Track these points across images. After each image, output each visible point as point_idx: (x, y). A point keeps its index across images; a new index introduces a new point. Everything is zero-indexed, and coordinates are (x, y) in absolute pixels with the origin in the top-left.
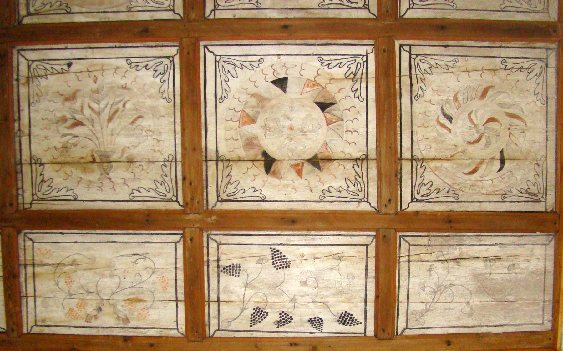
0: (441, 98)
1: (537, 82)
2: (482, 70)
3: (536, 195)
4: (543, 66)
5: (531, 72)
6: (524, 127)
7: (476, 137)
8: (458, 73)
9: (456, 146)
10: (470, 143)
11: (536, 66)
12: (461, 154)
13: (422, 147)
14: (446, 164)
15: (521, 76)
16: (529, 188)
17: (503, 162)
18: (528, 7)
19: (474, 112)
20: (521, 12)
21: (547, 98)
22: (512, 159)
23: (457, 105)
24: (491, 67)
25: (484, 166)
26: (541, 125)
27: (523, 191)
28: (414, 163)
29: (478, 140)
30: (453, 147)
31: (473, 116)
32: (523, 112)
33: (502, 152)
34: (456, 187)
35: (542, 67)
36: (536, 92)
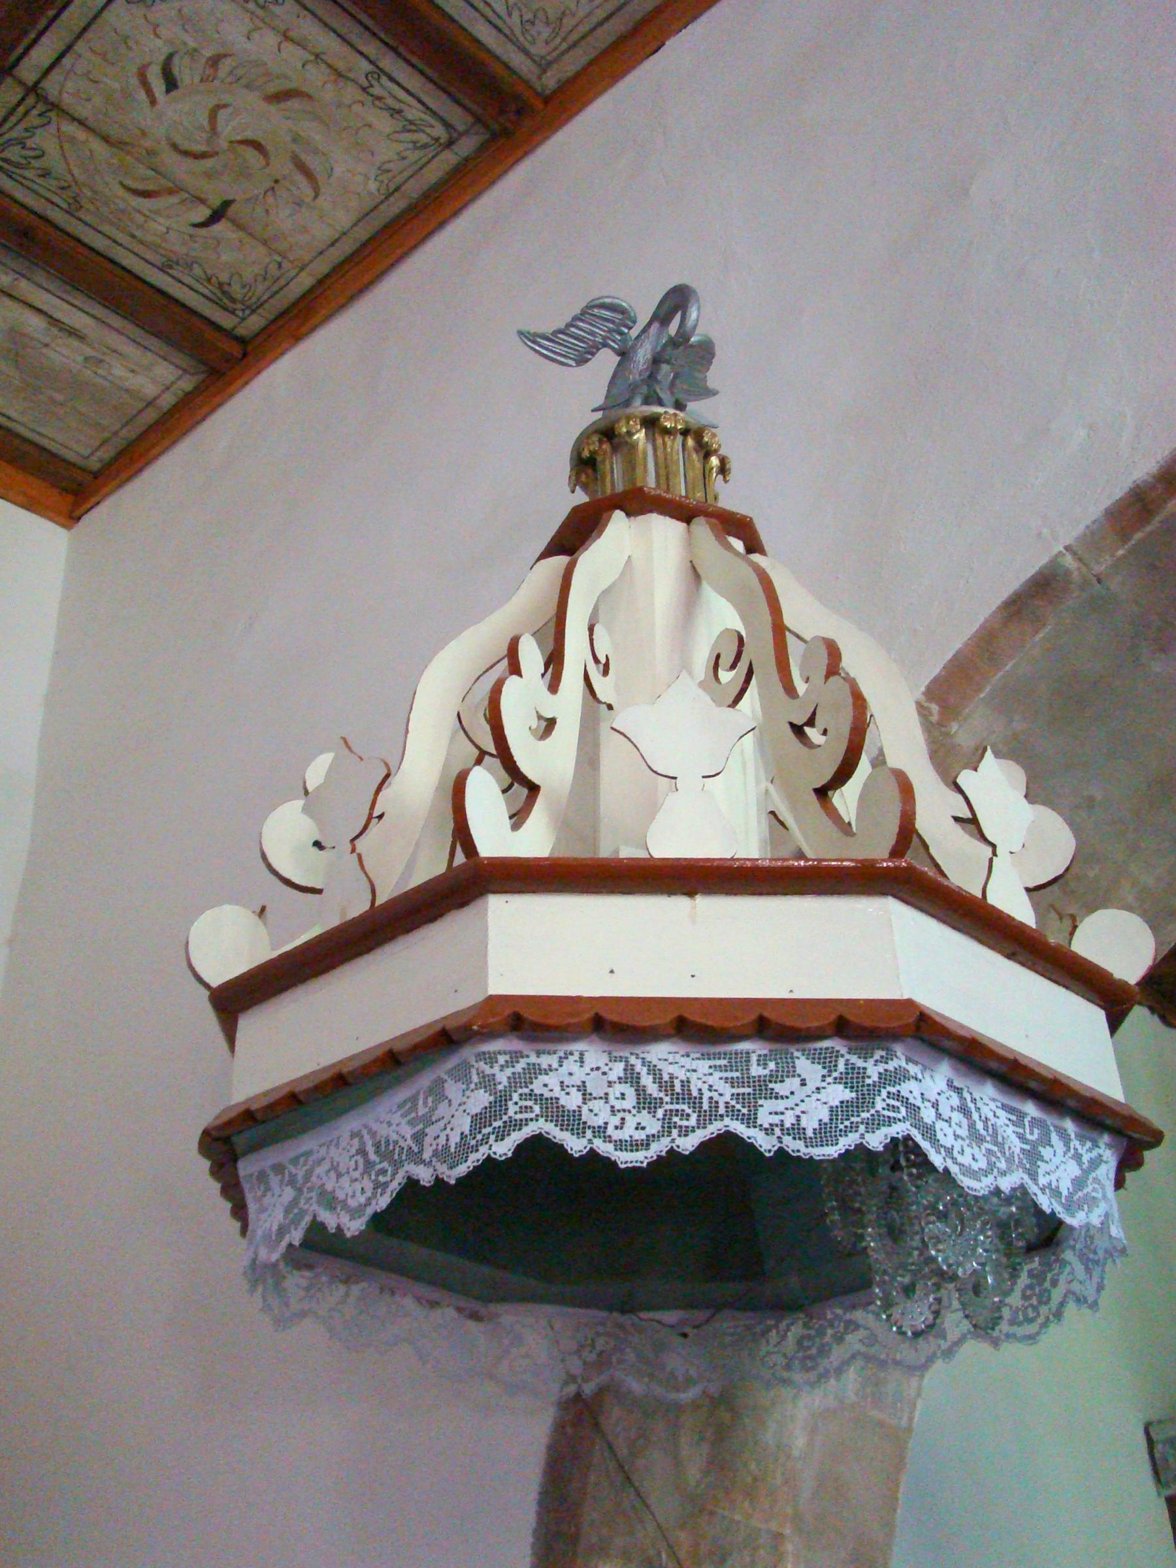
0: (185, 37)
1: (404, 154)
2: (317, 56)
3: (234, 301)
4: (442, 141)
5: (409, 131)
6: (308, 200)
7: (202, 148)
8: (261, 25)
9: (144, 134)
10: (175, 147)
11: (428, 130)
12: (144, 152)
13: (70, 86)
14: (97, 145)
15: (384, 124)
16: (229, 284)
17: (216, 216)
18: (517, 30)
19: (230, 110)
20: (496, 27)
21: (397, 189)
22: (238, 226)
23: (207, 72)
24: (341, 65)
25: (173, 200)
26: (343, 219)
27: (214, 280)
28: (31, 100)
29: (203, 156)
30: (138, 132)
31: (222, 115)
32: (330, 176)
33: (227, 204)
34: (86, 190)
35: (437, 140)
36: (387, 166)
